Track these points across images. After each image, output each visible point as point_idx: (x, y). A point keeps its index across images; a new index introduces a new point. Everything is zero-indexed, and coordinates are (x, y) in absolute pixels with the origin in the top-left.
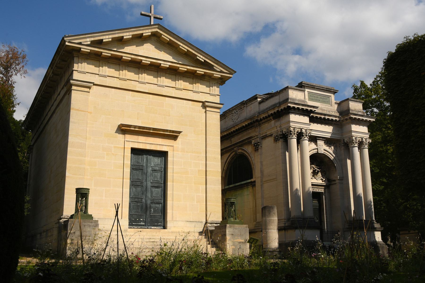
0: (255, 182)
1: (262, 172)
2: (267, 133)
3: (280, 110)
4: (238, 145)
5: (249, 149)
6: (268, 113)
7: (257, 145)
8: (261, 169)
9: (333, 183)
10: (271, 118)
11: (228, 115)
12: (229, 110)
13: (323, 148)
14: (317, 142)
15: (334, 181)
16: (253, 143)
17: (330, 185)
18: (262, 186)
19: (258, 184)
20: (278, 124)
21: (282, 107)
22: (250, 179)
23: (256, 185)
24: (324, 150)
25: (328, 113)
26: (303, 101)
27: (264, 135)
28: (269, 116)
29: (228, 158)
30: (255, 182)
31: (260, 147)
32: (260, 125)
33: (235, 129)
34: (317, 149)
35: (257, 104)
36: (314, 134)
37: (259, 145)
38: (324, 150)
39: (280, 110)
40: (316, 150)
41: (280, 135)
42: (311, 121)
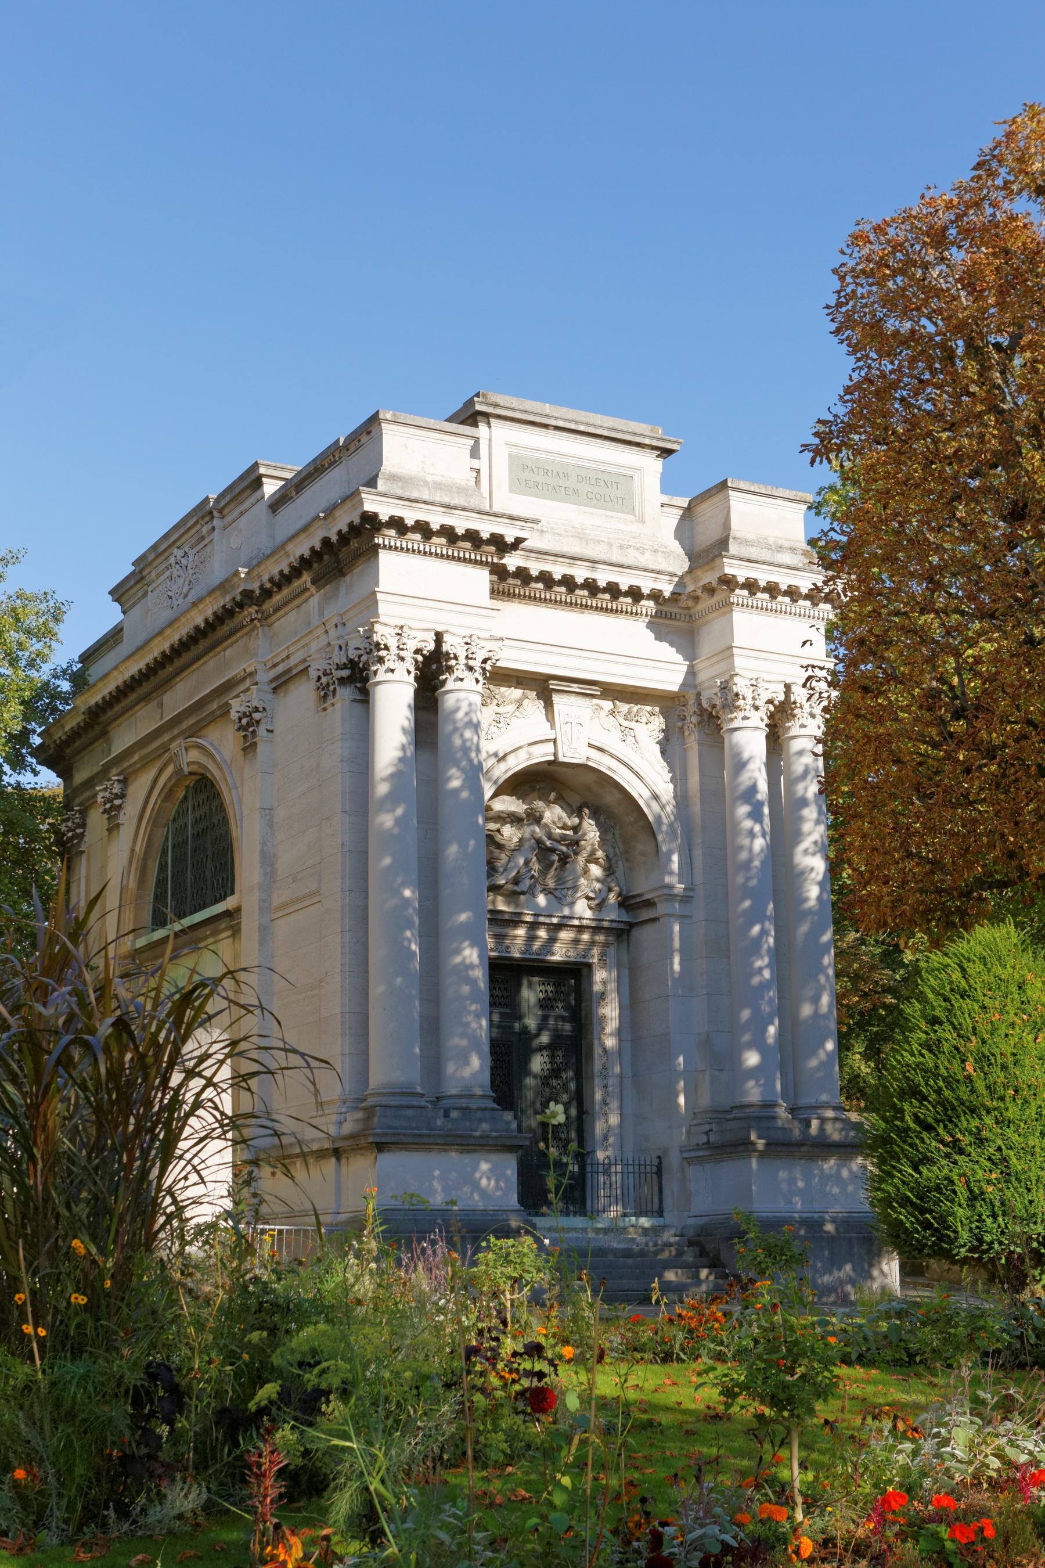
0: (238, 909)
1: (268, 860)
2: (292, 662)
3: (334, 538)
4: (185, 725)
5: (223, 741)
6: (287, 555)
7: (248, 725)
8: (264, 843)
9: (645, 914)
10: (306, 578)
11: (153, 575)
12: (154, 547)
13: (583, 734)
14: (549, 705)
15: (650, 904)
16: (234, 715)
17: (631, 925)
18: (265, 932)
19: (249, 922)
20: (332, 612)
21: (342, 522)
22: (222, 898)
23: (243, 927)
24: (590, 745)
25: (616, 557)
26: (461, 490)
27: (280, 669)
28: (296, 572)
29: (152, 788)
30: (238, 909)
31: (261, 731)
32: (265, 618)
33: (166, 646)
34: (555, 741)
35: (262, 509)
36: (511, 659)
37: (258, 722)
38: (590, 745)
39: (334, 538)
40: (549, 748)
41: (339, 667)
42: (495, 593)
